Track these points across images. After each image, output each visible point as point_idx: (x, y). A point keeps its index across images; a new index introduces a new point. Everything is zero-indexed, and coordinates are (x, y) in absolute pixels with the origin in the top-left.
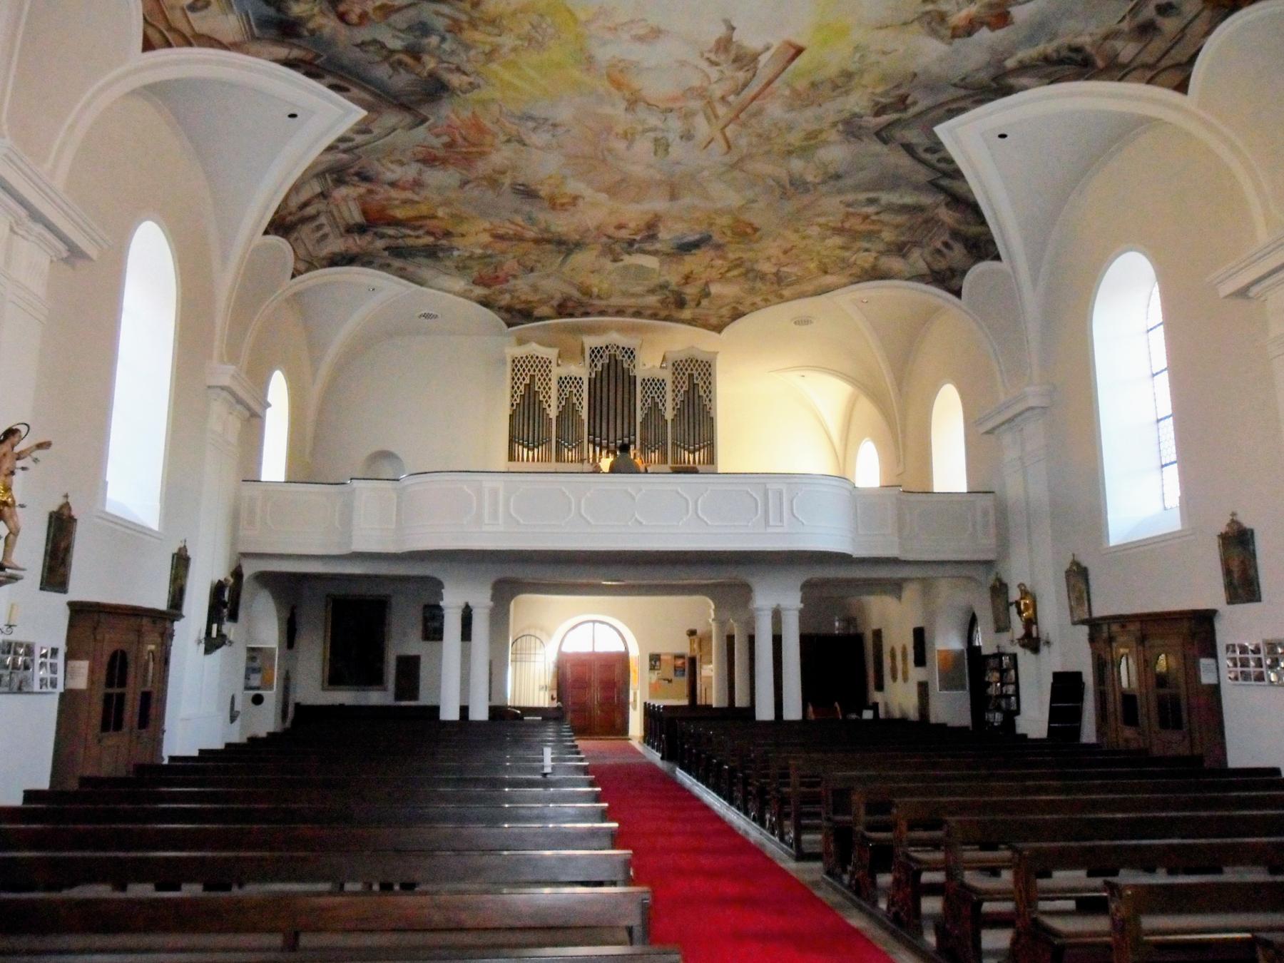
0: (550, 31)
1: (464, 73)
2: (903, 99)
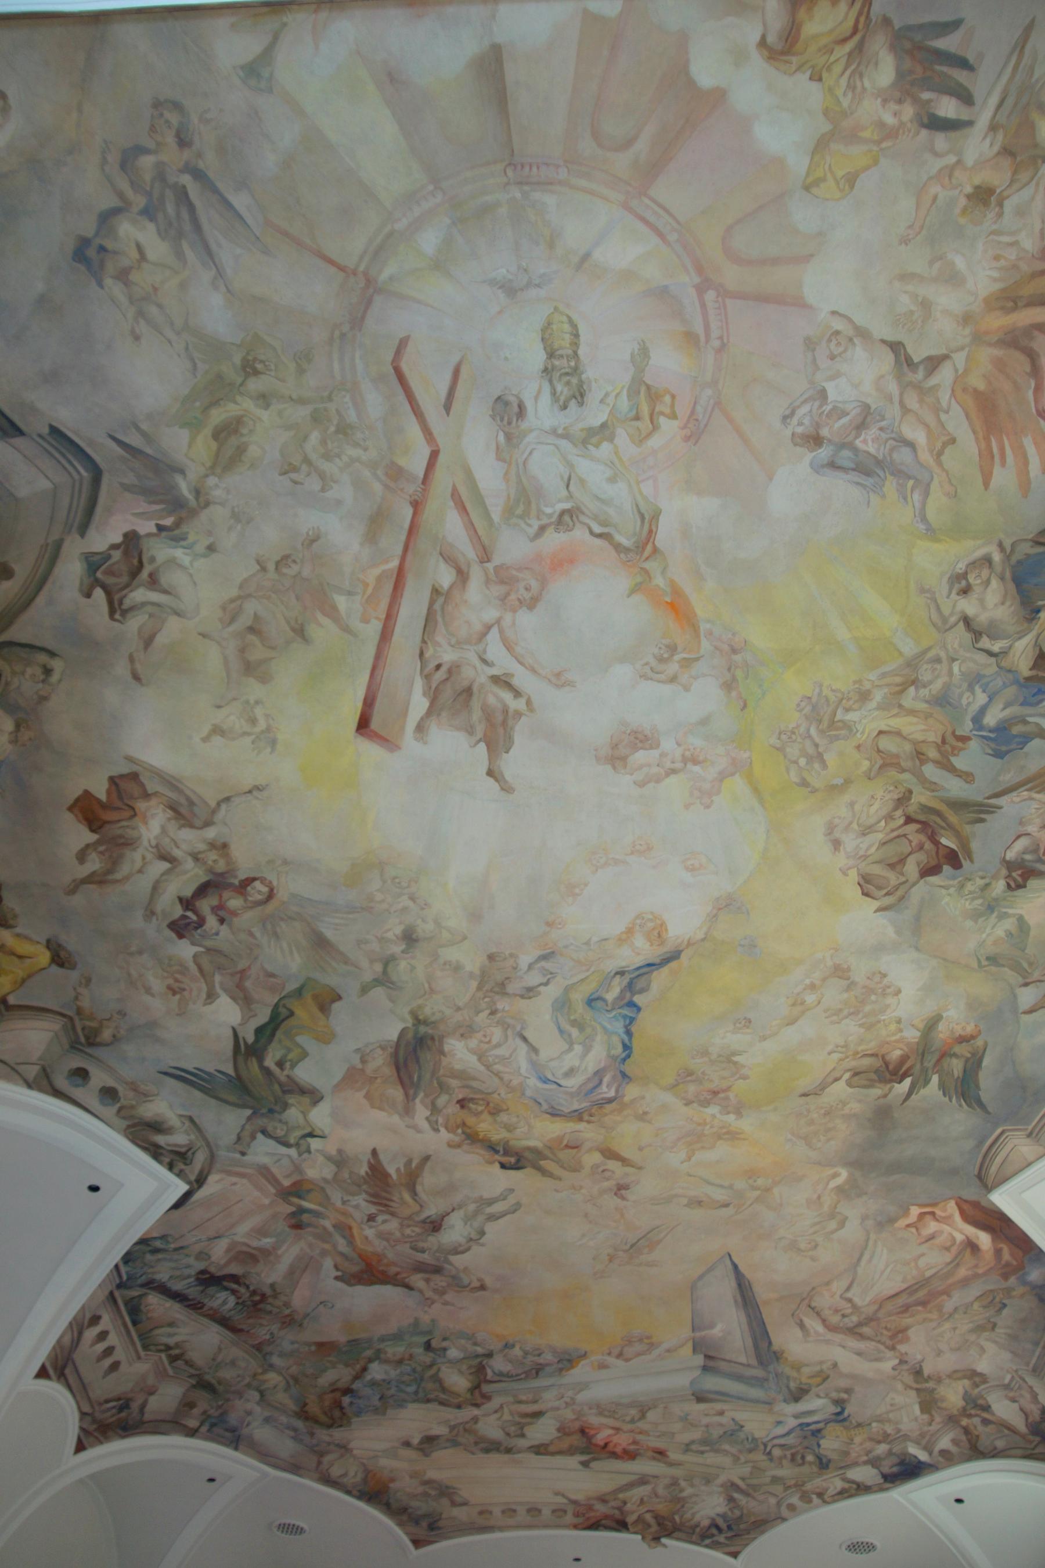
0: (793, 751)
1: (967, 621)
2: (116, 609)
